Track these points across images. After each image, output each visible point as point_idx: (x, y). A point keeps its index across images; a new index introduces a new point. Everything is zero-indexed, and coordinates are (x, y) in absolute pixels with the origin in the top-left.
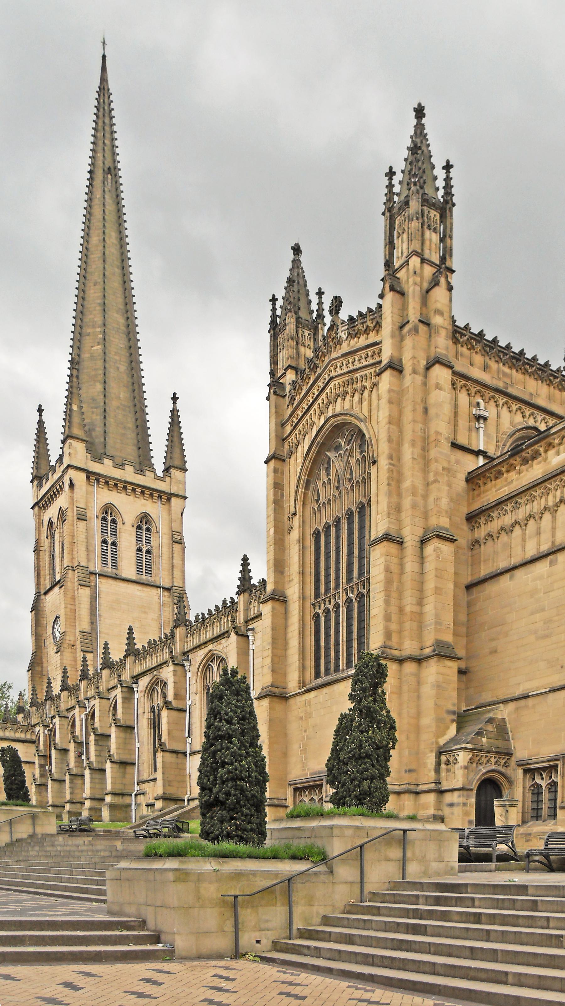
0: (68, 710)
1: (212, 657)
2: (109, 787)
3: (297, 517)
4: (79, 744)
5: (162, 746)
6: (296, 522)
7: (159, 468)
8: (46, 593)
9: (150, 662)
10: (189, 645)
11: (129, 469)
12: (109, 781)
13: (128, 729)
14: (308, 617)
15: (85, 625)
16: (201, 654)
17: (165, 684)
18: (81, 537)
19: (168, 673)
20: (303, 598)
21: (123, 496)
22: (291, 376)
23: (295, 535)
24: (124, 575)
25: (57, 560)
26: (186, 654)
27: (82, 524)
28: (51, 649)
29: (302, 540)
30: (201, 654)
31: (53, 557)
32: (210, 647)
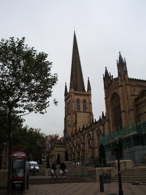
0: (73, 140)
1: (98, 129)
2: (81, 156)
3: (110, 107)
4: (75, 147)
5: (90, 147)
6: (110, 108)
7: (86, 91)
8: (67, 116)
9: (88, 130)
10: (94, 127)
11: (81, 92)
12: (81, 155)
13: (84, 144)
14: (113, 123)
15: (74, 122)
16: (96, 129)
17: (91, 135)
18: (73, 105)
19: (91, 132)
20: (112, 120)
21: (80, 96)
22: (107, 86)
23: (110, 110)
24: (81, 111)
25: (69, 110)
26: (94, 129)
27: (73, 103)
28: (68, 127)
29: (111, 111)
30: (96, 129)
31: (68, 109)
32: (98, 128)
